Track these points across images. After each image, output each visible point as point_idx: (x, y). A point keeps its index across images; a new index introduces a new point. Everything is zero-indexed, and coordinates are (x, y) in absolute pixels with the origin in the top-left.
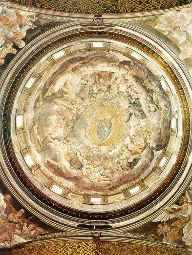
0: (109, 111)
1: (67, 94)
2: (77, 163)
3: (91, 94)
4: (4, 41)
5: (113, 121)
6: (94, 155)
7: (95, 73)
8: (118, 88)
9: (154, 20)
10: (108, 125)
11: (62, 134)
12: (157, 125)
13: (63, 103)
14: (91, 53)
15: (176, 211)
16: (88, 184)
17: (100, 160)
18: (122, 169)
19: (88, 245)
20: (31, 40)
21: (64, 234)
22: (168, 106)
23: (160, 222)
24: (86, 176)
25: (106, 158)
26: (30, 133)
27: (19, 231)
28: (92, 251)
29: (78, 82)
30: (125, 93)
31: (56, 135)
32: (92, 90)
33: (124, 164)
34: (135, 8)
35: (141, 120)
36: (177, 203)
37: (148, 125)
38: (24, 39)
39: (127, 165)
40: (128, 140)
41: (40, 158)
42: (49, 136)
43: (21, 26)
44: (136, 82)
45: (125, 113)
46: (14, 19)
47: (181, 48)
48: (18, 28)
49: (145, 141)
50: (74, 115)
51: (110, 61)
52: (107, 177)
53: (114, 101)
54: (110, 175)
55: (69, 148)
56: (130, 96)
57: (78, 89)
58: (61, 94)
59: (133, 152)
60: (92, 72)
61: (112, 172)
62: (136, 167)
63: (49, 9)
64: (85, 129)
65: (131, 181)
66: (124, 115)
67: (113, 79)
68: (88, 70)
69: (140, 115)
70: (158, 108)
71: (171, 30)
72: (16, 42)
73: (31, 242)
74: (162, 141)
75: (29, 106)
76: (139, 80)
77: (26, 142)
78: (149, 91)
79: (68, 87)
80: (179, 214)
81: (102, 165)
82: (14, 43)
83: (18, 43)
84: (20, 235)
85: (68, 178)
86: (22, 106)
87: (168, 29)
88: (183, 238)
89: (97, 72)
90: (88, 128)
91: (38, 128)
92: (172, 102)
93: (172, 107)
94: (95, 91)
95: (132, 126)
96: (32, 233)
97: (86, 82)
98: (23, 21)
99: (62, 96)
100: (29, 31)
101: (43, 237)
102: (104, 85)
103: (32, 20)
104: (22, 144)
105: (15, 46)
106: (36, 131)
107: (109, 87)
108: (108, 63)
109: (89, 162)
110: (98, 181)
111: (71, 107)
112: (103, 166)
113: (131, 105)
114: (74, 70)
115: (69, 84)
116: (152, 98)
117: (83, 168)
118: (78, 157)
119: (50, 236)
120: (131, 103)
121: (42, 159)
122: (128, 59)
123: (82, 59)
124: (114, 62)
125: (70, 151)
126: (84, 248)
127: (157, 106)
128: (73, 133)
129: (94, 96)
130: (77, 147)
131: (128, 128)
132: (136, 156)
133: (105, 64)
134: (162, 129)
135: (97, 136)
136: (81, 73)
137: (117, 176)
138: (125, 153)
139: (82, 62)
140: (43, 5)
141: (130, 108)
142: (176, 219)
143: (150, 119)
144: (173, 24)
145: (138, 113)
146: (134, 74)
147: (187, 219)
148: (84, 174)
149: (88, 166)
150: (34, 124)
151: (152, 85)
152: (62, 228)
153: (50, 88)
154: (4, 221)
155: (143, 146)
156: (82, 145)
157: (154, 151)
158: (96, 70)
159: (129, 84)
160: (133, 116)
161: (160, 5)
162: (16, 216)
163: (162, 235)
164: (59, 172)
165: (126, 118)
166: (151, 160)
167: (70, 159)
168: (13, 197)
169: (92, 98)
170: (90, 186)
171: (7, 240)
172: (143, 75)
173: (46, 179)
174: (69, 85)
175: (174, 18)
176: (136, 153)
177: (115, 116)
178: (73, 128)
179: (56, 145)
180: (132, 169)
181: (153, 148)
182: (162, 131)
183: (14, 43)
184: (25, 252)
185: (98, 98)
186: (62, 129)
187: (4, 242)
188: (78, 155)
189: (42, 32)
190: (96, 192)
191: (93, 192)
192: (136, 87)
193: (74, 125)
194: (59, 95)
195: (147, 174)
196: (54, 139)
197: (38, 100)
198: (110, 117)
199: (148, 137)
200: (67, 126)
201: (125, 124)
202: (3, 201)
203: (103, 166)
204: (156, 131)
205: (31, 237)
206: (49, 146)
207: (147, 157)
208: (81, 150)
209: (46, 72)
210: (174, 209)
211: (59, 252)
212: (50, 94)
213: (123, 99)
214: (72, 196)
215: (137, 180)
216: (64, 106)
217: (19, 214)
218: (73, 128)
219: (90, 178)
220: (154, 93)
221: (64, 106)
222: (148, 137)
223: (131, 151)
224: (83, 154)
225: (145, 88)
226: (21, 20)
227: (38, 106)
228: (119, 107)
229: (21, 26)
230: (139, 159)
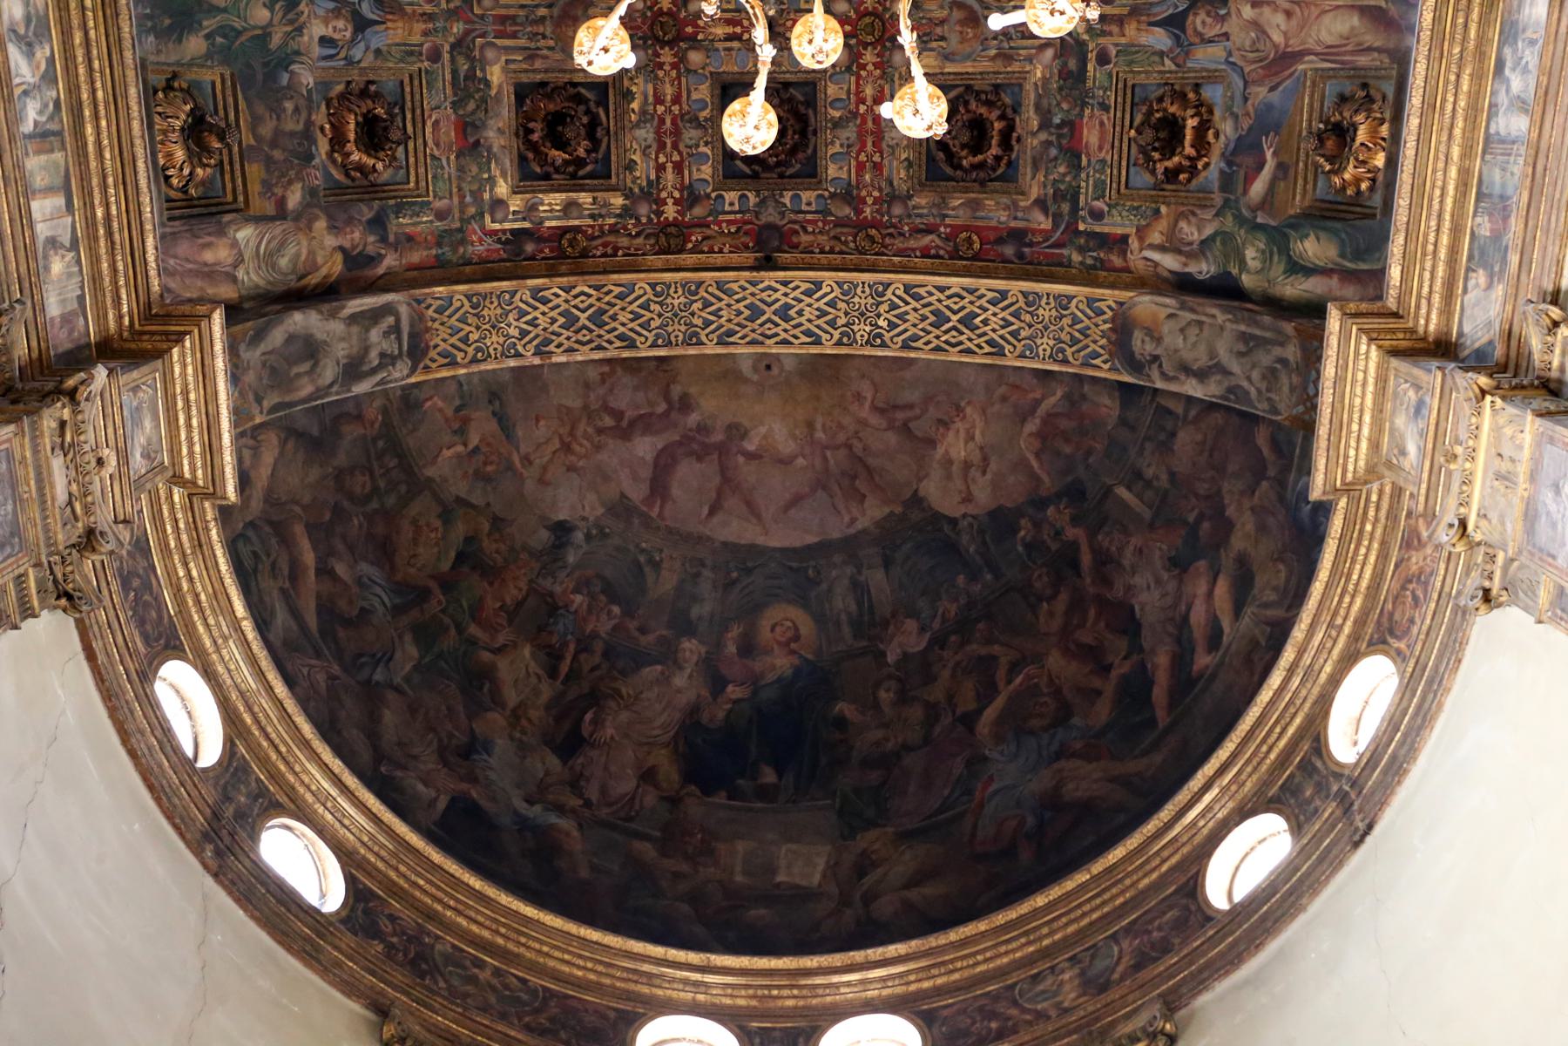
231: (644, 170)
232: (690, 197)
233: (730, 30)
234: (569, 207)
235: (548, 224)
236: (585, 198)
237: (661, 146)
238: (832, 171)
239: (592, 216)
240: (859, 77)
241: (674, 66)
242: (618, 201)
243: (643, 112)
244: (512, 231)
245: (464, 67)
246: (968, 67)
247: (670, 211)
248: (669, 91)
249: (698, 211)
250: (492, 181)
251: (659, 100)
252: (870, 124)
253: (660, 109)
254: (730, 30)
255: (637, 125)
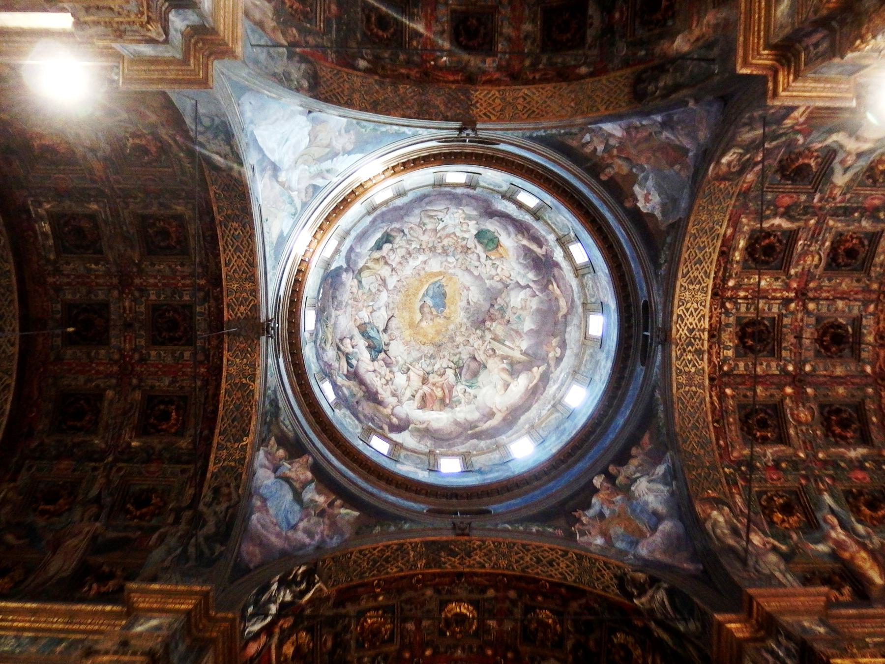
0: (425, 336)
1: (504, 369)
2: (486, 241)
3: (459, 369)
4: (633, 488)
5: (418, 316)
6: (454, 256)
7: (452, 408)
8: (409, 379)
9: (360, 528)
10: (426, 310)
11: (513, 294)
12: (338, 313)
13: (510, 353)
14: (461, 449)
15: (320, 174)
16: (467, 205)
17: (443, 247)
18: (403, 231)
19: (485, 114)
20: (583, 489)
21: (528, 134)
22: (321, 351)
23: (349, 153)
24: (469, 218)
25: (433, 249)
26: (573, 301)
27: (612, 142)
28: (477, 102)
29: (484, 390)
30: (395, 369)
31: (523, 294)
32: (456, 375)
33: (399, 240)
34: (397, 550)
35: (367, 320)
36: (316, 188)
37: (354, 313)
38: (595, 491)
39: (394, 237)
40: (392, 282)
41: (555, 255)
42: (537, 293)
43: (601, 515)
44: (377, 393)
45: (396, 333)
46: (617, 530)
47: (309, 475)
48: (607, 513)
49: (360, 282)
50: (489, 329)
51: (426, 432)
52: (431, 217)
53: (415, 354)
54: (426, 220)
55: (499, 269)
56: (388, 365)
57: (483, 377)
58: (514, 369)
59: (382, 262)
60: (458, 409)
61: (422, 224)
62: (378, 235)
63: (552, 549)
64: (469, 303)
65: (389, 211)
66: (398, 328)
67: (418, 396)
68: (464, 413)
69: (369, 330)
70: (337, 345)
71: (331, 511)
72: (609, 485)
73: (591, 124)
74: (331, 285)
75: (575, 350)
76: (372, 397)
77: (582, 286)
78: (354, 375)
79: (501, 383)
80: (314, 169)
81: (440, 238)
82: (614, 484)
83: (605, 484)
84: (610, 135)
85: (504, 217)
86: (588, 352)
87: (336, 511)
88: (310, 128)
89: (448, 409)
90: (464, 304)
91: (558, 309)
92: (315, 360)
93: (314, 349)
94: (450, 373)
95: (383, 309)
96: (587, 137)
97: (468, 390)
98: (598, 524)
99: (512, 364)
100: (588, 505)
101: (567, 130)
102: (434, 384)
103: (581, 527)
104: (590, 283)
105: (611, 478)
106: (562, 303)
107: (425, 381)
108: (429, 427)
109: (464, 242)
110: (448, 209)
111: (496, 345)
112: (438, 235)
113: (385, 348)
114: (491, 415)
115: (499, 387)
116: (348, 363)
117: (475, 232)
118: (485, 252)
119: (554, 131)
120: (385, 352)
121: (552, 251)
122: (395, 436)
123: (478, 436)
124: (418, 430)
125: (498, 263)
126: (494, 109)
127: (339, 349)
128: (493, 296)
129: (451, 364)
130: (484, 271)
131: (391, 306)
132: (377, 255)
133: (435, 425)
134: (330, 303)
135: (447, 289)
136: (477, 408)
137: (413, 220)
138: (398, 259)
139: (477, 430)
140: (562, 556)
141: (387, 342)
142: (320, 160)
143: (352, 323)
144: (327, 521)
145: (373, 333)
146: (381, 408)
147: (300, 160)
148: (474, 222)
149: (466, 235)
150: (565, 316)
151: (348, 388)
152: (530, 144)
153: (535, 382)
154: (640, 162)
155: (365, 274)
156: (476, 273)
157: (345, 266)
158: (450, 414)
159: (390, 388)
160: (381, 328)
161: (353, 557)
162: (620, 167)
163: (347, 131)
164: (521, 228)
165: (393, 324)
166: (351, 249)
167: (500, 249)
168: (621, 203)
169: (456, 359)
170: (464, 201)
171: (636, 128)
172: (367, 408)
173: (546, 218)
174: (500, 385)
175: (325, 533)
176: (377, 260)
177: (412, 325)
178: (492, 305)
179: (524, 276)
180: (386, 232)
181: (347, 270)
182: (330, 303)
183: (614, 484)
184: (604, 107)
185: (445, 360)
186: (512, 304)
187: (642, 125)
188: (483, 256)
189: (563, 503)
190: (454, 191)
191: (459, 191)
192: (375, 382)
193: (489, 311)
194: (518, 367)
195: (359, 225)
196: (528, 286)
197: (559, 360)
198: (424, 324)
199: (355, 290)
200: (502, 310)
201: (396, 313)
202: (640, 198)
203: (438, 235)
204: (340, 303)
205: (592, 131)
206: (537, 275)
207: (357, 255)
208: (477, 264)
209: (544, 412)
210: (323, 178)
211: (541, 102)
212: (535, 369)
213: (399, 358)
214: (500, 187)
215: (378, 212)
216: (510, 348)
217: (610, 171)
218: (492, 305)
219: (463, 216)
220: (345, 372)
221: (510, 348)
222: (355, 290)
223: (386, 263)
224: (475, 257)
225: (362, 382)
226: (601, 528)
227: (558, 351)
228: (407, 344)
229: (601, 515)
230: (372, 250)
231: (67, 269)
232: (58, 289)
233: (127, 308)
234: (45, 234)
235: (36, 225)
236: (51, 242)
237: (78, 277)
238: (69, 352)
239: (43, 245)
240: (107, 364)
241: (112, 284)
242: (52, 257)
243: (91, 269)
244: (29, 209)
245: (92, 193)
246: (105, 411)
247: (51, 280)
248: (101, 281)
249: (52, 292)
250: (49, 202)
251: (97, 277)
252: (88, 369)
253: (93, 277)
254: (127, 308)
255: (85, 267)
